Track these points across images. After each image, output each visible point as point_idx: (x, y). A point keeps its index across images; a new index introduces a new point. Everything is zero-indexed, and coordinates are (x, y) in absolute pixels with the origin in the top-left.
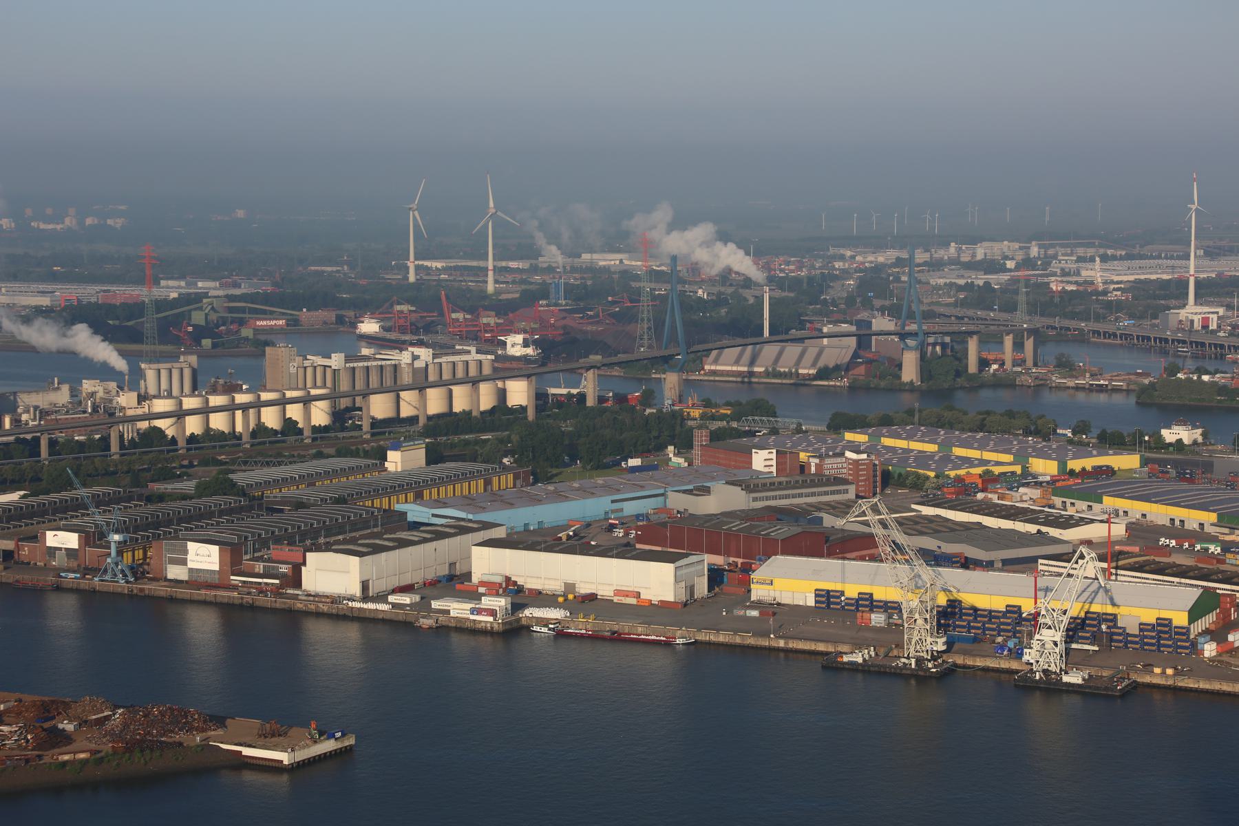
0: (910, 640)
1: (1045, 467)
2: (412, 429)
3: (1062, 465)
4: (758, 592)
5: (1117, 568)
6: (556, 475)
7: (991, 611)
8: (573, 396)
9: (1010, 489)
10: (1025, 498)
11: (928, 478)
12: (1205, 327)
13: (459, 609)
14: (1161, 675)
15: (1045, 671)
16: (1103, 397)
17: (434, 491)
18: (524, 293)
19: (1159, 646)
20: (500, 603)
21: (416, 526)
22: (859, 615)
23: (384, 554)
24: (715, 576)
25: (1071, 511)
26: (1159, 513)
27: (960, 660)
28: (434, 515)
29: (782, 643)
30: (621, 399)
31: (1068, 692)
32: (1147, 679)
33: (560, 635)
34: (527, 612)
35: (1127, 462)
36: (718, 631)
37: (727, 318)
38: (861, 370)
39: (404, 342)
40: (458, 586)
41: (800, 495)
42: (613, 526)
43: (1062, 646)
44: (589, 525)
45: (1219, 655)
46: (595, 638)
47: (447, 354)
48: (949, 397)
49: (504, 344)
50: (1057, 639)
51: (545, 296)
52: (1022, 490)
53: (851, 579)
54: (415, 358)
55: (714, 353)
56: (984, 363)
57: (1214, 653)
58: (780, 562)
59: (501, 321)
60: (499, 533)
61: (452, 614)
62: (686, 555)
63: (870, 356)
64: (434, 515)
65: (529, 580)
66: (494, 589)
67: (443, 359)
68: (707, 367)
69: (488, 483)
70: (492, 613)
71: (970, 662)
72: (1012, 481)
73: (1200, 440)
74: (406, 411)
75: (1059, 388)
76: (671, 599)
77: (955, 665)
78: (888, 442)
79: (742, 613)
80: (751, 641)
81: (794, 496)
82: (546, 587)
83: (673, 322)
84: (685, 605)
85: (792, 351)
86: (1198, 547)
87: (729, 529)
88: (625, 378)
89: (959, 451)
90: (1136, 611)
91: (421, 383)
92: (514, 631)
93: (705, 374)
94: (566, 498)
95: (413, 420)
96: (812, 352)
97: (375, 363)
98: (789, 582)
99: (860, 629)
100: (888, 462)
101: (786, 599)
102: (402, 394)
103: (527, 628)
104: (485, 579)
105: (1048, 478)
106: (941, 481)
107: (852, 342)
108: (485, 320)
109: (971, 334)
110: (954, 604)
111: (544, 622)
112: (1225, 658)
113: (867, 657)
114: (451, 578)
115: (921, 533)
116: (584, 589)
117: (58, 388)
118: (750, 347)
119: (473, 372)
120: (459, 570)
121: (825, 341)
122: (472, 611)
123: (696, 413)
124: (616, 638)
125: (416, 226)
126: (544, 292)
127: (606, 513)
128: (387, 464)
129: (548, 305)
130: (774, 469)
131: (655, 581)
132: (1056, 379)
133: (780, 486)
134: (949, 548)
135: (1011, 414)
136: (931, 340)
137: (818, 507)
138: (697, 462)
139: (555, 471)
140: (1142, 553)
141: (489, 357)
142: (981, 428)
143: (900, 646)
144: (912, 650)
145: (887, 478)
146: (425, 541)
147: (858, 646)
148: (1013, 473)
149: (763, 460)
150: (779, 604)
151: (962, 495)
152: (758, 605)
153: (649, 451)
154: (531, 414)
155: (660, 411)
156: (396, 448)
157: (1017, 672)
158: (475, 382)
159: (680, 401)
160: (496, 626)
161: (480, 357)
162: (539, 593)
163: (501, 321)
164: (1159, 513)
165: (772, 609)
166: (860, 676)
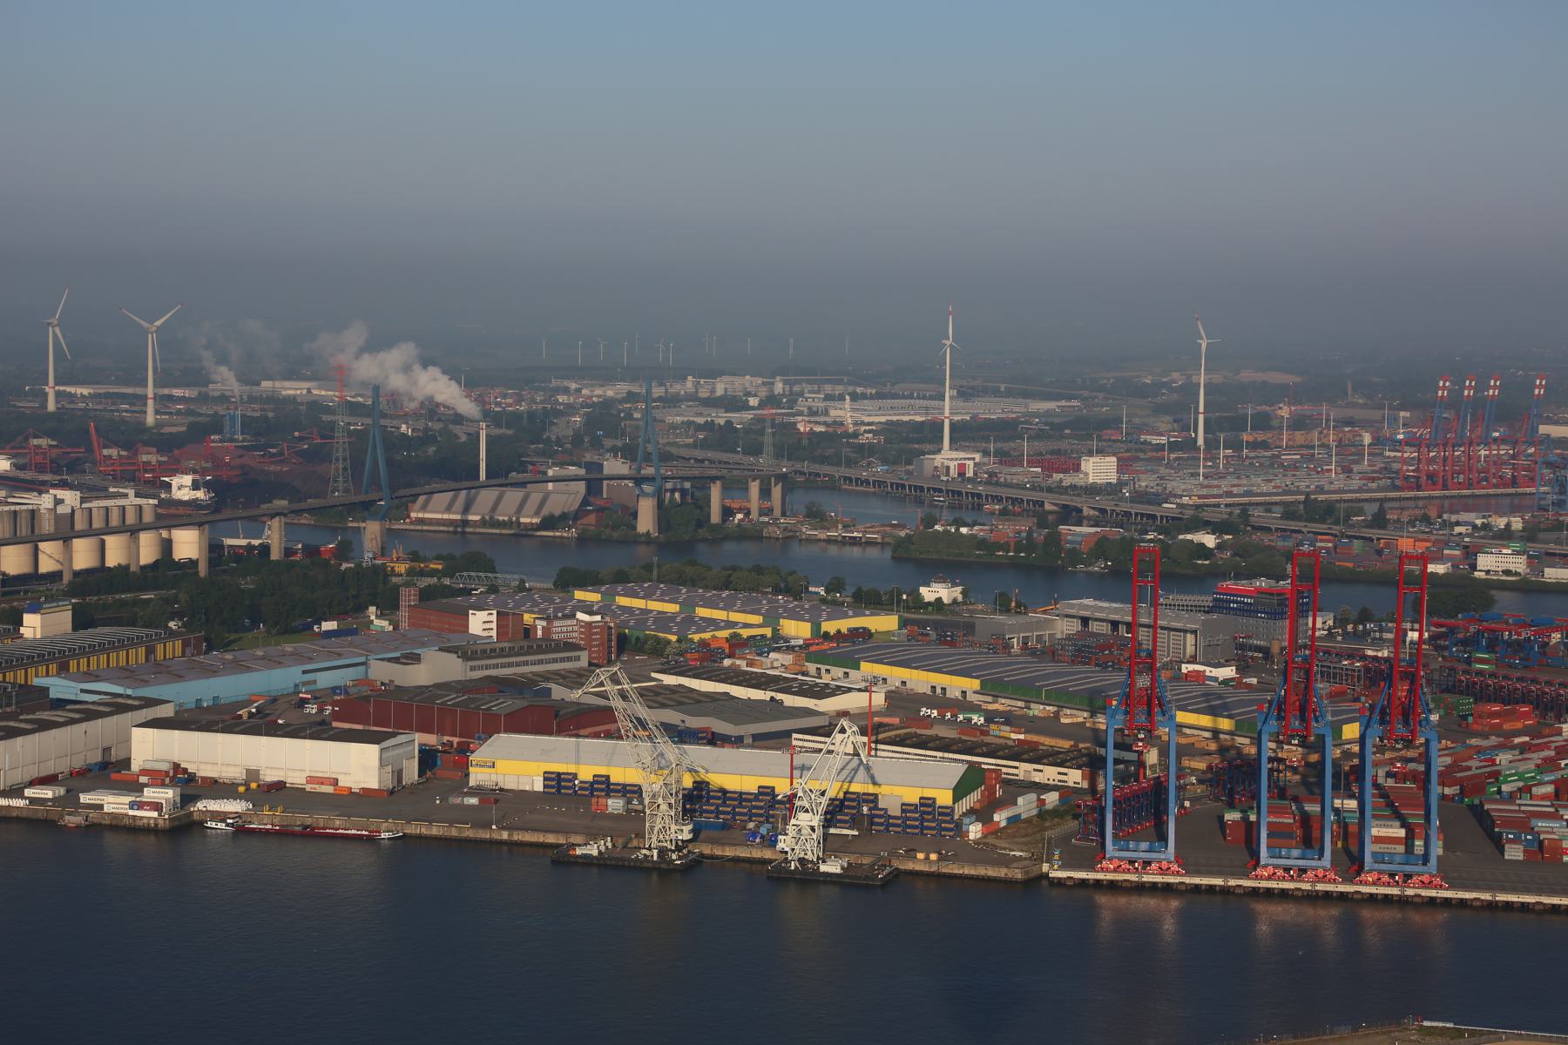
0: (652, 828)
1: (797, 630)
2: (55, 587)
3: (816, 627)
4: (477, 776)
5: (877, 742)
6: (235, 641)
7: (741, 794)
8: (254, 547)
9: (760, 655)
10: (776, 664)
11: (669, 642)
12: (962, 474)
13: (114, 803)
14: (923, 861)
15: (801, 860)
16: (856, 551)
17: (84, 662)
18: (192, 426)
19: (923, 828)
20: (166, 795)
21: (60, 704)
22: (594, 800)
23: (19, 740)
24: (427, 758)
25: (826, 679)
26: (920, 680)
27: (707, 850)
28: (83, 691)
29: (505, 835)
30: (312, 552)
31: (825, 882)
32: (910, 866)
33: (241, 831)
34: (200, 805)
35: (884, 623)
36: (431, 822)
37: (438, 459)
38: (592, 519)
39: (44, 483)
40: (114, 776)
41: (526, 663)
42: (304, 701)
43: (819, 832)
44: (275, 700)
45: (985, 836)
46: (284, 834)
47: (98, 498)
48: (689, 550)
49: (169, 485)
50: (815, 823)
51: (219, 431)
52: (772, 655)
53: (585, 759)
54: (58, 502)
55: (422, 499)
56: (727, 512)
57: (979, 835)
58: (503, 740)
59: (164, 459)
60: (167, 711)
61: (106, 809)
62: (394, 735)
63: (601, 503)
64: (83, 691)
65: (202, 766)
66: (158, 778)
67: (94, 504)
68: (413, 515)
69: (150, 651)
70: (157, 807)
71: (718, 852)
72: (763, 646)
73: (960, 598)
74: (46, 566)
75: (811, 540)
76: (375, 786)
77: (702, 855)
78: (623, 601)
79: (458, 800)
80: (470, 833)
81: (518, 664)
82: (224, 774)
83: (375, 462)
84: (392, 792)
85: (513, 496)
86: (961, 717)
87: (444, 703)
88: (315, 527)
89: (702, 612)
90: (898, 791)
91: (66, 532)
92: (184, 827)
93: (412, 523)
94: (248, 669)
95: (55, 576)
96: (535, 498)
97: (7, 508)
98: (514, 764)
99: (595, 816)
100: (625, 624)
101: (510, 784)
102: (42, 545)
103: (200, 824)
104: (149, 766)
105: (801, 642)
106: (684, 646)
107: (581, 487)
108: (145, 458)
109: (714, 479)
110: (700, 786)
111: (221, 817)
112: (991, 840)
113: (603, 849)
114: (105, 766)
115: (663, 706)
116: (270, 776)
118: (464, 493)
119: (131, 519)
120: (115, 755)
121: (550, 485)
122: (132, 805)
123: (401, 568)
124: (309, 834)
125: (57, 344)
126: (216, 425)
127: (296, 686)
128: (22, 630)
129: (221, 441)
130: (494, 633)
131: (356, 765)
132: (807, 531)
133: (502, 653)
134: (694, 722)
135: (758, 570)
136: (669, 485)
137: (547, 677)
138: (404, 625)
139: (233, 636)
140: (902, 725)
141: (151, 501)
142: (726, 585)
143: (640, 835)
144: (654, 840)
145: (623, 644)
146: (73, 722)
147: (593, 836)
148: (763, 636)
149: (481, 623)
150: (501, 790)
151: (707, 662)
152: (478, 791)
153: (346, 613)
154: (203, 569)
155: (359, 565)
156: (34, 610)
157: (770, 861)
158: (134, 532)
159: (383, 555)
160: (161, 822)
161: (139, 501)
162: (214, 781)
163: (164, 459)
164: (920, 680)
165: (494, 796)
166: (595, 871)
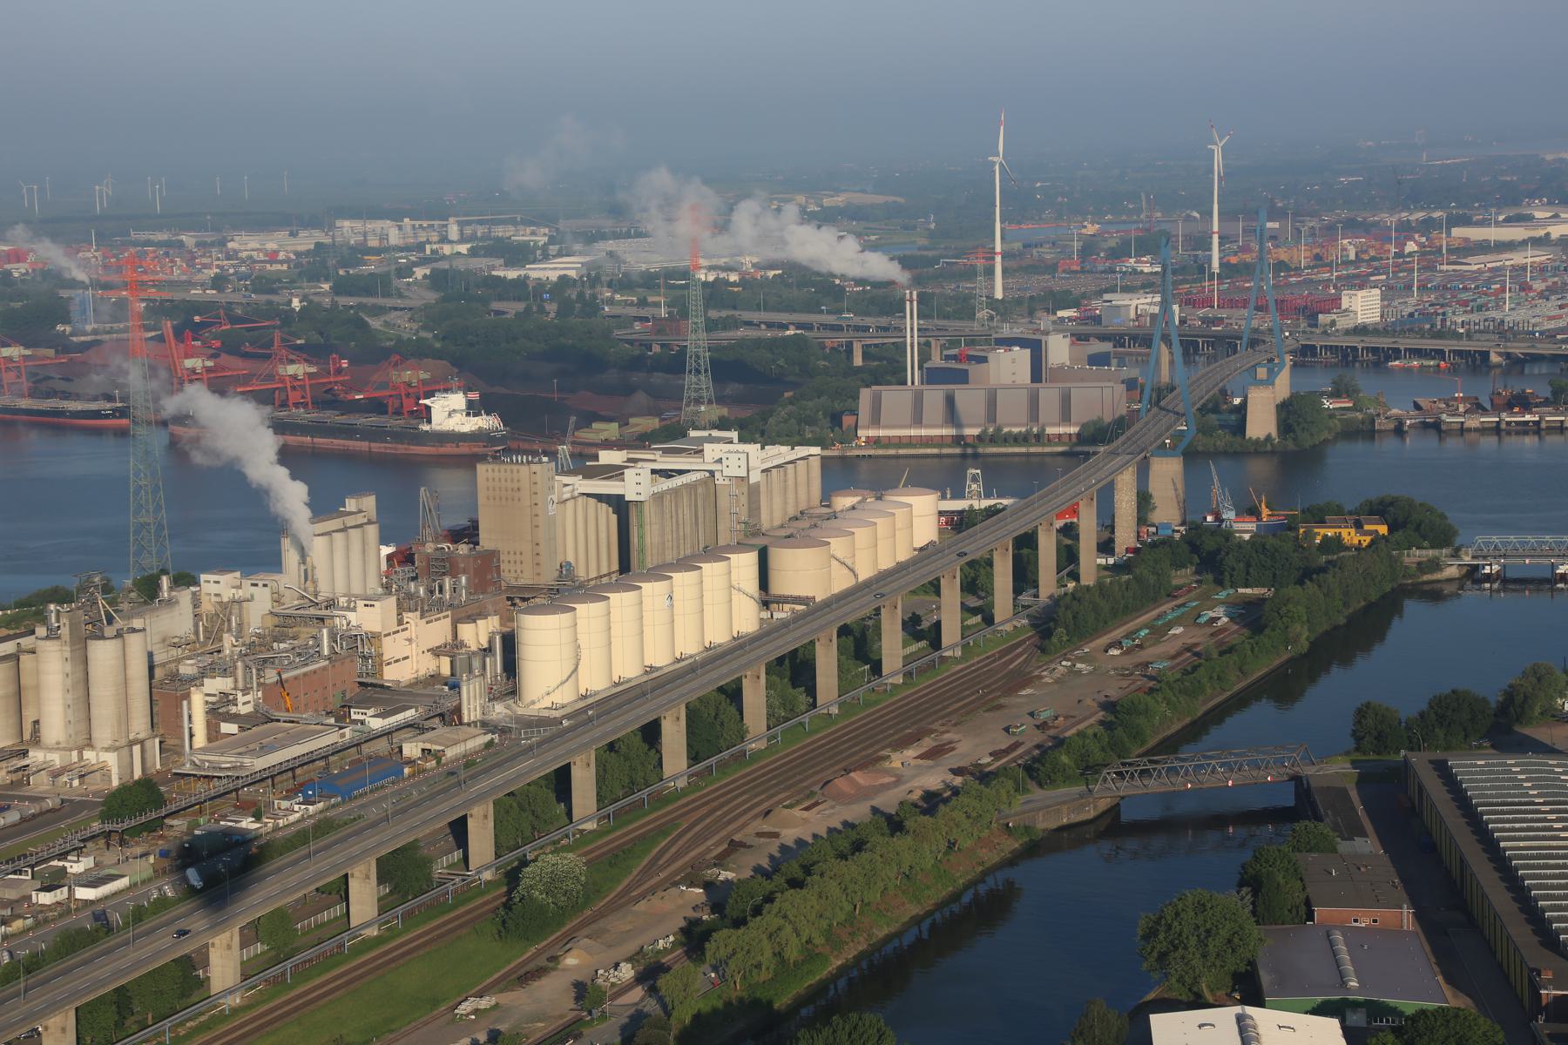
16: (1529, 441)
59: (313, 370)
68: (862, 433)
108: (292, 369)
117: (171, 603)
163: (313, 370)
